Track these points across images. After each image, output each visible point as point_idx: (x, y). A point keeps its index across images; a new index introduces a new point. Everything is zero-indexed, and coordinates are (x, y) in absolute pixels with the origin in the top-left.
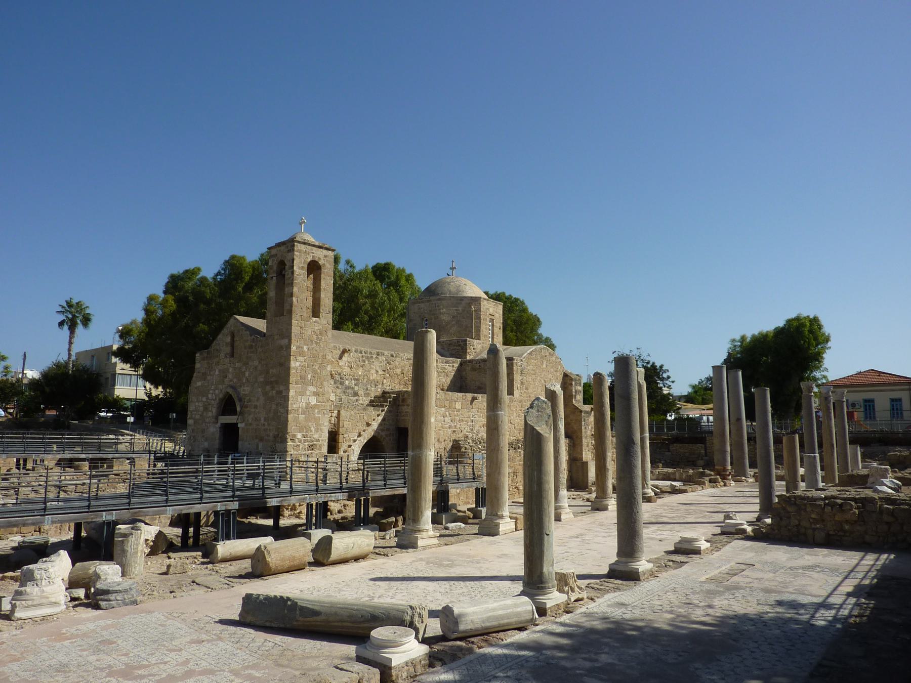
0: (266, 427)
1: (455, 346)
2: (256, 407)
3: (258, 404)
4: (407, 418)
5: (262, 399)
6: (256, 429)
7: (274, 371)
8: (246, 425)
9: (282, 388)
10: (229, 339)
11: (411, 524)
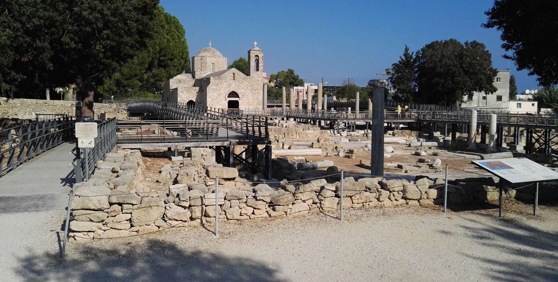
2: (248, 96)
5: (251, 94)
7: (256, 86)
9: (259, 91)
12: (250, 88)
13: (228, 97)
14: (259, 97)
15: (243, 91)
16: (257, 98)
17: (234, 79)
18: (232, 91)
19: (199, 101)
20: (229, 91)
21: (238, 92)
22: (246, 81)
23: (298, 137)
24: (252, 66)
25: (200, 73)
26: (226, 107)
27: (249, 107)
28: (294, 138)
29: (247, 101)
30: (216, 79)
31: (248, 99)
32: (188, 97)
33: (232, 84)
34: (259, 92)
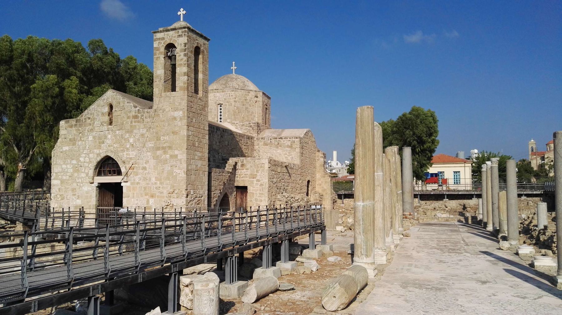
0: (158, 185)
1: (247, 126)
2: (144, 168)
3: (147, 166)
4: (246, 179)
5: (152, 162)
6: (145, 188)
7: (166, 138)
8: (132, 184)
9: (176, 152)
10: (107, 109)
11: (365, 258)
15: (133, 154)
18: (103, 155)
22: (142, 125)
24: (157, 76)
27: (148, 202)
29: (143, 184)
30: (71, 127)
31: (145, 179)
33: (106, 137)
34: (176, 156)
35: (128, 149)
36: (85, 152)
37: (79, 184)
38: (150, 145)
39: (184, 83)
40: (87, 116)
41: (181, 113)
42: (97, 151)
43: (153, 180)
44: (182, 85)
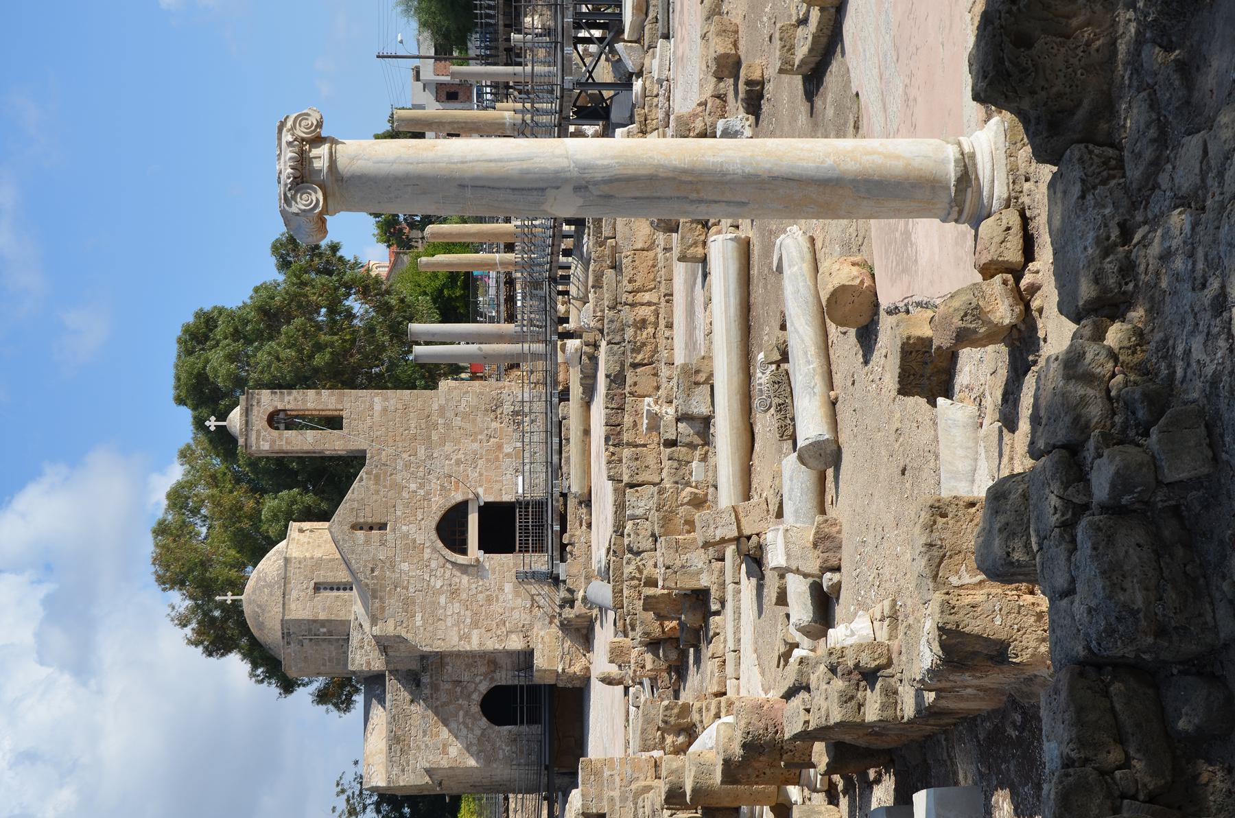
2: (458, 462)
5: (448, 447)
6: (488, 460)
8: (481, 486)
9: (435, 407)
10: (360, 534)
12: (422, 452)
13: (464, 552)
14: (461, 409)
15: (435, 485)
16: (465, 416)
17: (382, 527)
18: (434, 535)
19: (483, 669)
20: (435, 550)
21: (438, 505)
23: (647, 297)
25: (362, 647)
26: (503, 564)
27: (508, 455)
28: (652, 319)
30: (383, 609)
31: (474, 461)
32: (469, 721)
33: (406, 536)
35: (428, 493)
36: (427, 577)
37: (480, 589)
38: (423, 452)
39: (333, 395)
40: (368, 574)
41: (376, 399)
42: (427, 553)
43: (476, 446)
44: (333, 399)
